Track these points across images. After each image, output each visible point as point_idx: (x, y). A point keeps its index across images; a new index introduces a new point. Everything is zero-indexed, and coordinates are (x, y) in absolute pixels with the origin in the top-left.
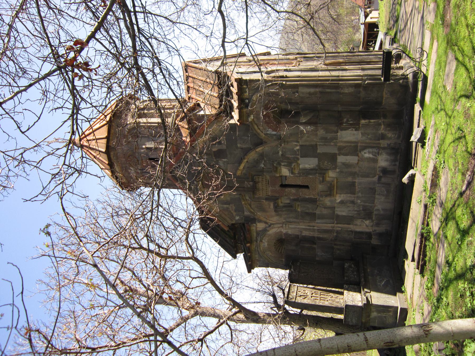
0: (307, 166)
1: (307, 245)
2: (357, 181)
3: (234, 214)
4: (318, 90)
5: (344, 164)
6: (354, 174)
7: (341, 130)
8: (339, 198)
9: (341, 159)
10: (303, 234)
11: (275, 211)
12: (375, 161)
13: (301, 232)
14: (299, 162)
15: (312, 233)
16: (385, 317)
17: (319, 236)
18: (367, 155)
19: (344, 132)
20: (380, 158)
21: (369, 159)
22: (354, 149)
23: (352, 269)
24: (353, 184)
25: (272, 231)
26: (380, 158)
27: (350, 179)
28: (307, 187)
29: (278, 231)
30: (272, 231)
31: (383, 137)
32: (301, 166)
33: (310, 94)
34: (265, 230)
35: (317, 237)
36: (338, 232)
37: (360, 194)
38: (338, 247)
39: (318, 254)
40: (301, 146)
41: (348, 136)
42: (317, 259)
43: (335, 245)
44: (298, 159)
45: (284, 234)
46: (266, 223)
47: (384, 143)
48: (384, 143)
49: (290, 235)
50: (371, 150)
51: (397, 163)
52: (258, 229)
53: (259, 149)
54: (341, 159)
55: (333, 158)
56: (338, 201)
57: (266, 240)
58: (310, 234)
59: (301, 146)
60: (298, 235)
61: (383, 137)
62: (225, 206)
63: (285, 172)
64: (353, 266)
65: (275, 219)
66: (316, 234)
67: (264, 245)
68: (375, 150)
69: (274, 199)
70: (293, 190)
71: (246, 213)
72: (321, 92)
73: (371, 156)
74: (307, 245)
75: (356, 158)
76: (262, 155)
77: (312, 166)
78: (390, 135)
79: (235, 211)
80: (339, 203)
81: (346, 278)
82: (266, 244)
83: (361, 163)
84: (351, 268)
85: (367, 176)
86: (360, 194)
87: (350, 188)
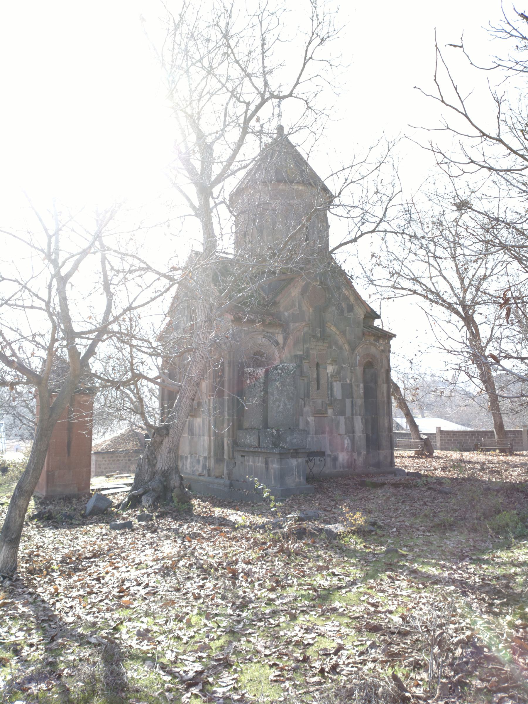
0: (335, 389)
2: (326, 435)
3: (290, 312)
4: (385, 399)
5: (339, 422)
6: (331, 432)
7: (362, 419)
8: (310, 419)
9: (342, 419)
11: (295, 356)
12: (342, 451)
14: (338, 382)
16: (293, 474)
18: (346, 442)
19: (360, 421)
20: (344, 453)
21: (343, 444)
22: (351, 431)
24: (323, 433)
26: (344, 453)
27: (327, 429)
28: (318, 389)
31: (359, 454)
32: (335, 384)
33: (383, 393)
34: (278, 344)
37: (315, 439)
40: (351, 385)
41: (359, 425)
44: (340, 381)
46: (284, 344)
47: (355, 456)
48: (355, 456)
50: (350, 445)
51: (342, 470)
52: (276, 335)
53: (346, 347)
54: (342, 419)
55: (342, 413)
56: (309, 419)
59: (351, 385)
61: (359, 454)
62: (297, 304)
63: (330, 369)
65: (286, 353)
68: (350, 449)
69: (306, 356)
70: (315, 376)
71: (292, 326)
72: (384, 402)
73: (346, 445)
75: (344, 433)
76: (341, 349)
77: (335, 393)
78: (361, 459)
79: (293, 313)
80: (307, 420)
83: (339, 437)
85: (330, 445)
86: (315, 439)
87: (319, 431)
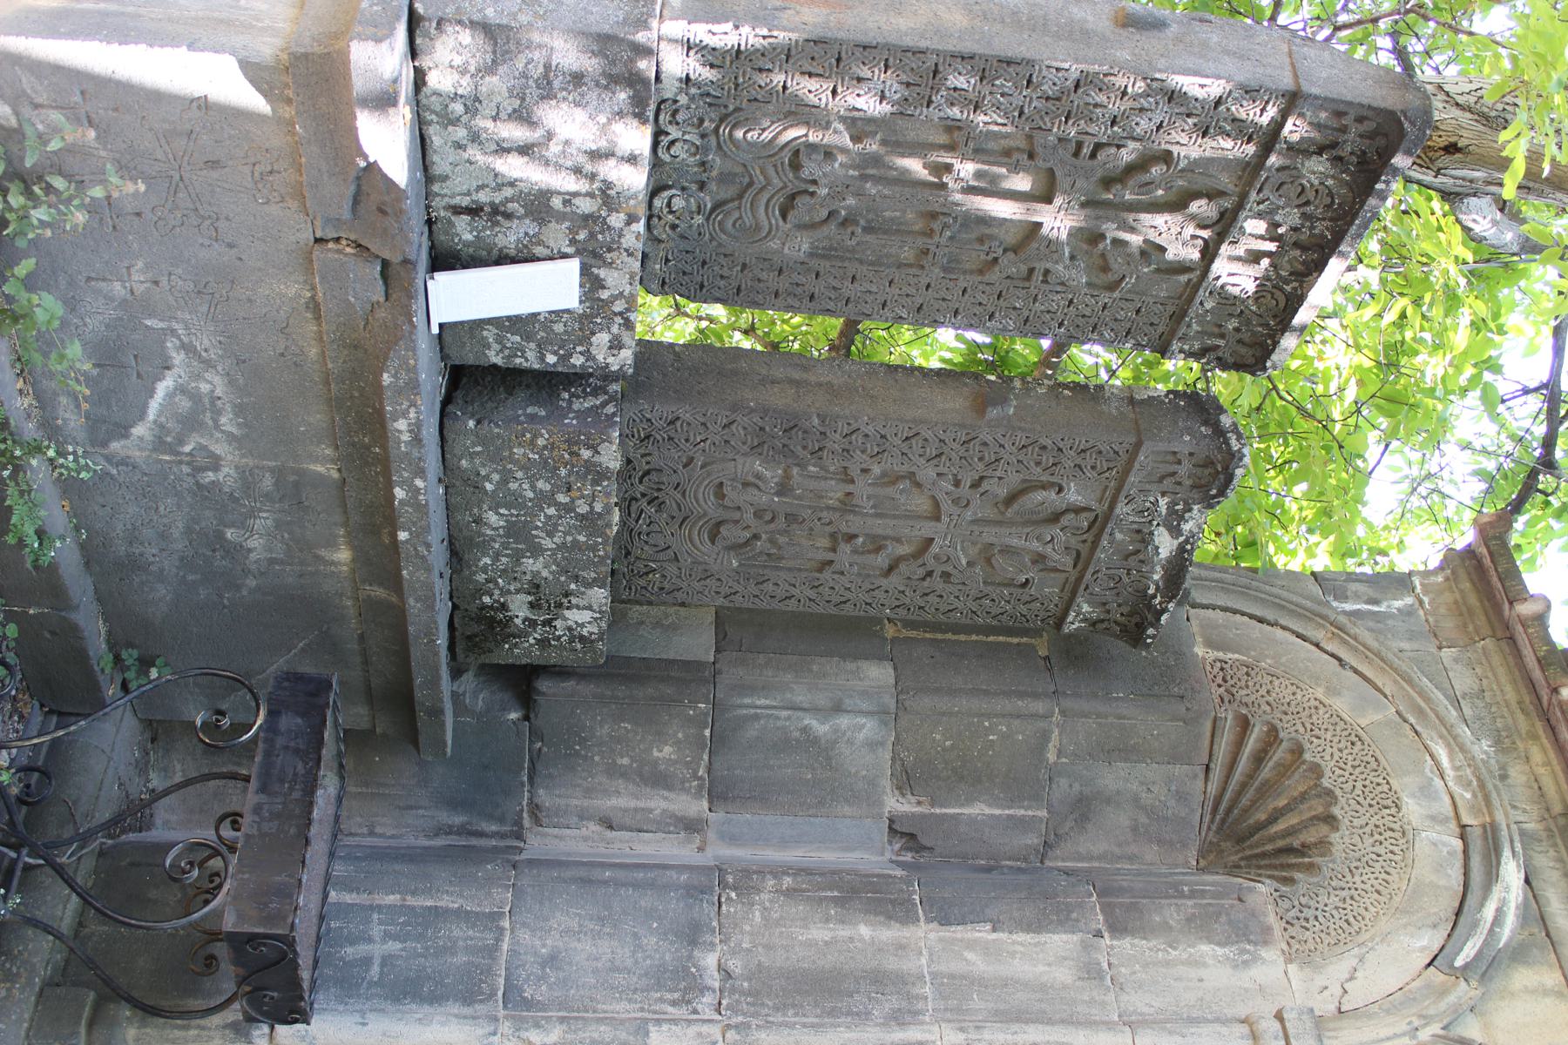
1: (979, 810)
10: (1060, 942)
13: (1092, 973)
15: (976, 963)
17: (890, 933)
23: (531, 564)
25: (1394, 956)
29: (1338, 969)
30: (1394, 956)
35: (909, 918)
36: (682, 984)
38: (659, 803)
39: (868, 728)
42: (879, 674)
43: (692, 826)
45: (1265, 936)
49: (1202, 925)
57: (1422, 846)
58: (987, 950)
60: (1117, 928)
64: (519, 608)
66: (922, 945)
67: (1425, 791)
74: (979, 810)
81: (611, 457)
82: (1413, 809)
84: (535, 587)
